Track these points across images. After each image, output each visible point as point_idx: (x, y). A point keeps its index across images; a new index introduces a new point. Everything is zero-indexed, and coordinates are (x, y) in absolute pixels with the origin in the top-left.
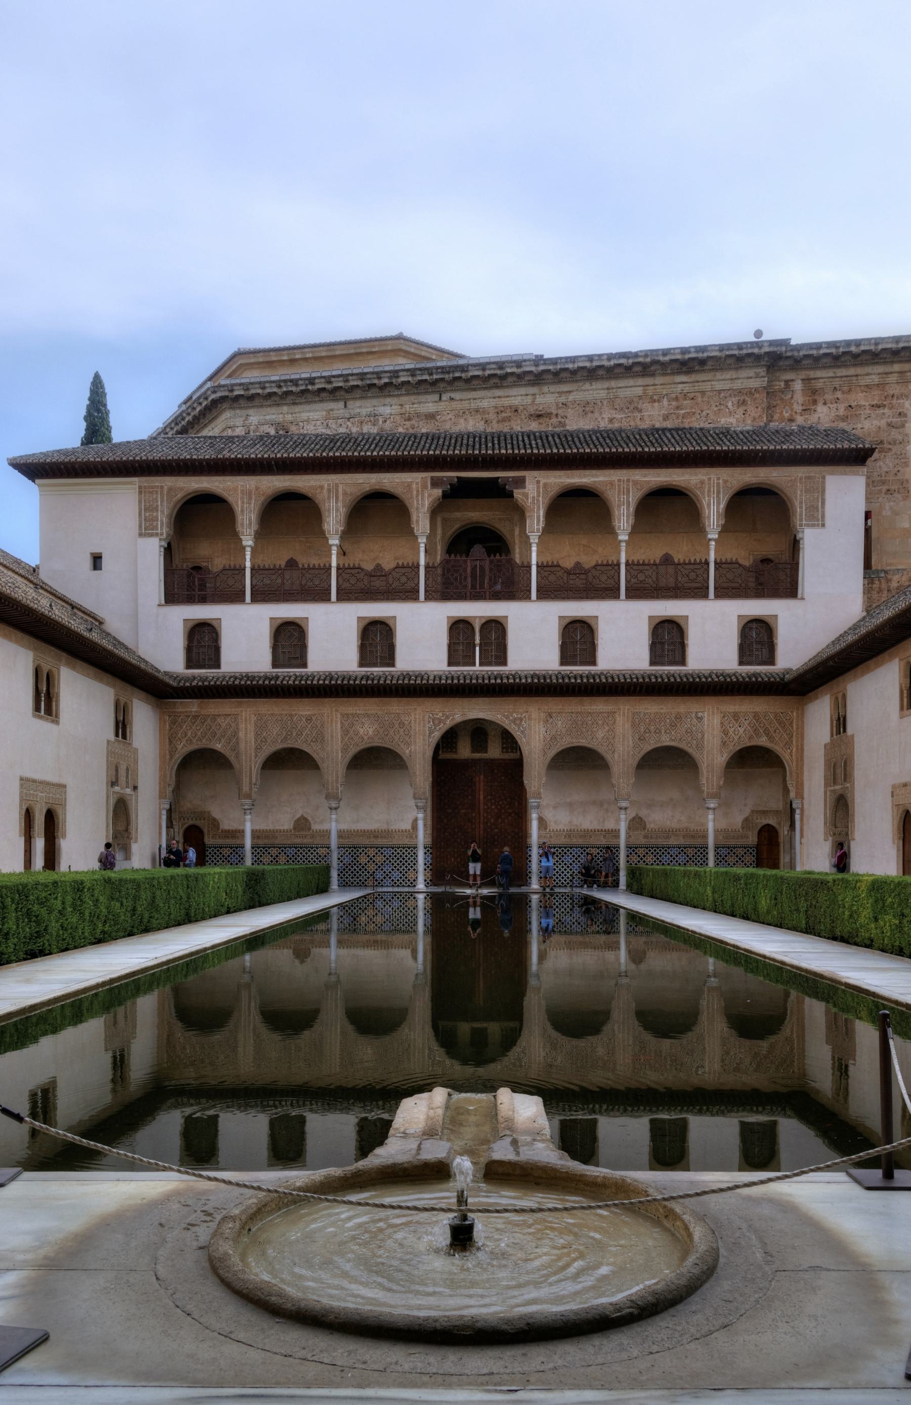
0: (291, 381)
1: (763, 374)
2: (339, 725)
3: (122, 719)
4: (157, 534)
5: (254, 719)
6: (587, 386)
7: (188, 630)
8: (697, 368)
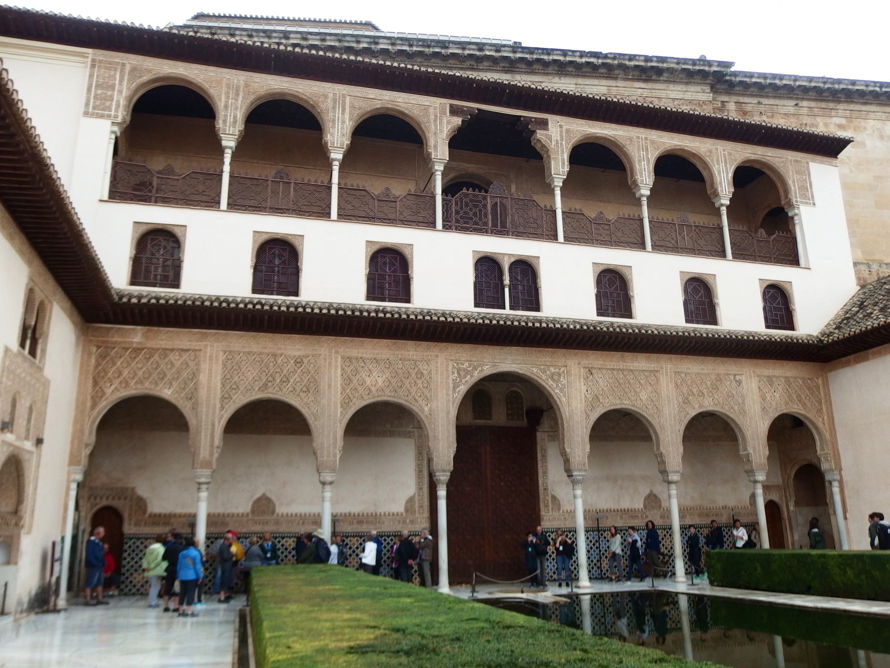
0: (264, 31)
1: (709, 91)
2: (339, 371)
3: (33, 323)
4: (109, 116)
5: (222, 357)
6: (556, 79)
7: (137, 235)
8: (654, 77)
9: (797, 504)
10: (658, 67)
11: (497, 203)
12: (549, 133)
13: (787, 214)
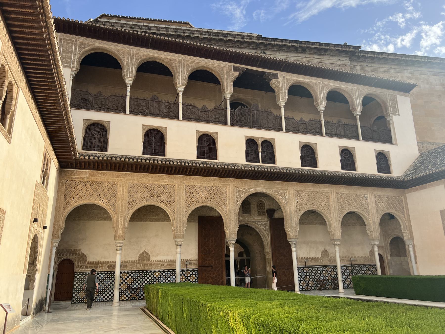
0: (138, 26)
1: (348, 60)
4: (70, 67)
6: (278, 53)
7: (86, 126)
9: (391, 256)
10: (325, 48)
11: (255, 113)
12: (279, 80)
13: (386, 119)
